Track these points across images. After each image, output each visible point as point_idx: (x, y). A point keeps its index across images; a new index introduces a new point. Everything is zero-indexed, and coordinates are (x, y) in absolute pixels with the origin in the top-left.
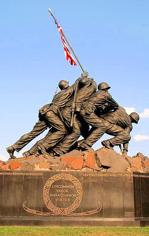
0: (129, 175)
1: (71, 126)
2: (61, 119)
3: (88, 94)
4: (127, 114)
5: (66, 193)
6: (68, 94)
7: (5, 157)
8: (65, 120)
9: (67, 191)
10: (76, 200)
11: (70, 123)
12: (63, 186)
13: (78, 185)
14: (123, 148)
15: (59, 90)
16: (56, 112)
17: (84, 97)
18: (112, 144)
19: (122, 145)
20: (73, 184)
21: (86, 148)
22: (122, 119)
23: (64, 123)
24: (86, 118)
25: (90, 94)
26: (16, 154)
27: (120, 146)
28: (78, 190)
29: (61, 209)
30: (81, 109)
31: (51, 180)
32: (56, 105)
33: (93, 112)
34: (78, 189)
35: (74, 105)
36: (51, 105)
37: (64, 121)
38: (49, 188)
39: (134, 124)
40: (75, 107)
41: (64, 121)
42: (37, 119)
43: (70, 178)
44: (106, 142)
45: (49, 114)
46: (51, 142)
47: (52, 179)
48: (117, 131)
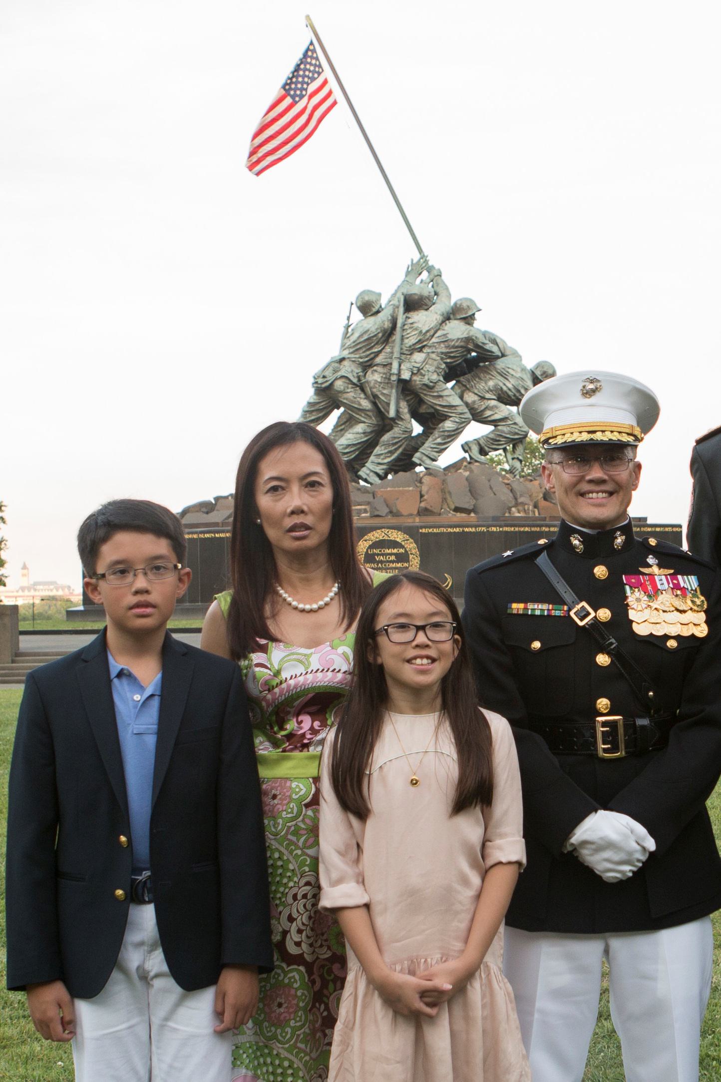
1: (392, 414)
2: (367, 397)
3: (427, 331)
4: (524, 369)
5: (393, 562)
6: (380, 335)
8: (375, 396)
9: (393, 558)
11: (388, 404)
12: (387, 551)
13: (411, 546)
15: (357, 316)
16: (355, 380)
17: (420, 340)
18: (487, 449)
19: (510, 448)
20: (402, 547)
22: (510, 386)
23: (374, 404)
24: (425, 395)
25: (432, 332)
27: (505, 450)
28: (411, 557)
30: (413, 374)
32: (354, 361)
33: (442, 379)
35: (395, 365)
36: (342, 360)
37: (374, 399)
40: (400, 366)
41: (374, 399)
42: (308, 394)
44: (471, 445)
45: (339, 385)
46: (347, 450)
48: (497, 417)
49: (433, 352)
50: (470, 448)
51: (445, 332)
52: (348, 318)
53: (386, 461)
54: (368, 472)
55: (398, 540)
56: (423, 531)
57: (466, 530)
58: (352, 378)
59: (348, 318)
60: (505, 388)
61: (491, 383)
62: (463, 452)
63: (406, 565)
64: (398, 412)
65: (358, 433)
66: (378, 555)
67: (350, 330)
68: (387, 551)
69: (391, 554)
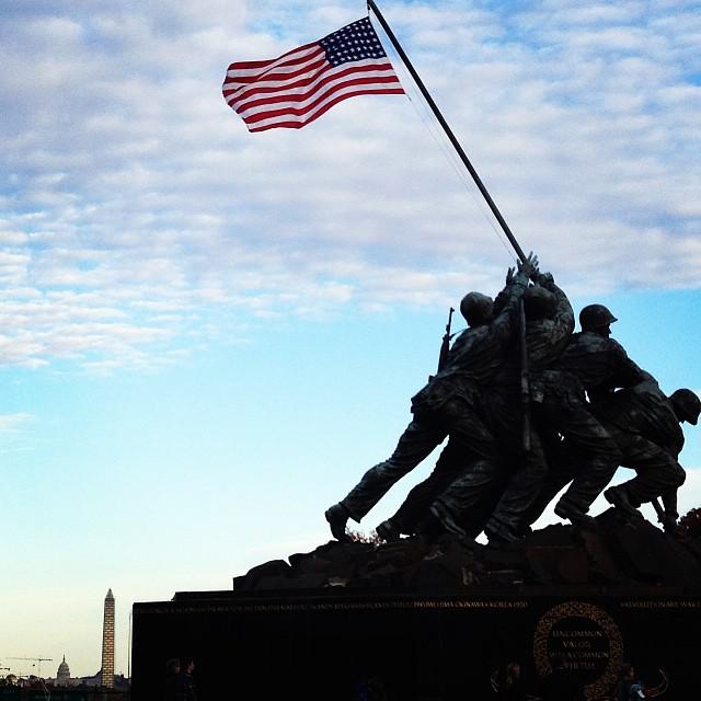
3: (557, 343)
7: (324, 535)
13: (610, 626)
20: (599, 628)
31: (549, 618)
35: (525, 384)
39: (685, 426)
43: (593, 613)
48: (647, 456)
49: (569, 370)
51: (581, 344)
52: (448, 328)
53: (518, 510)
54: (498, 525)
55: (593, 617)
58: (469, 400)
59: (448, 328)
60: (650, 420)
61: (633, 413)
62: (607, 502)
64: (531, 446)
65: (478, 472)
66: (565, 639)
67: (452, 343)
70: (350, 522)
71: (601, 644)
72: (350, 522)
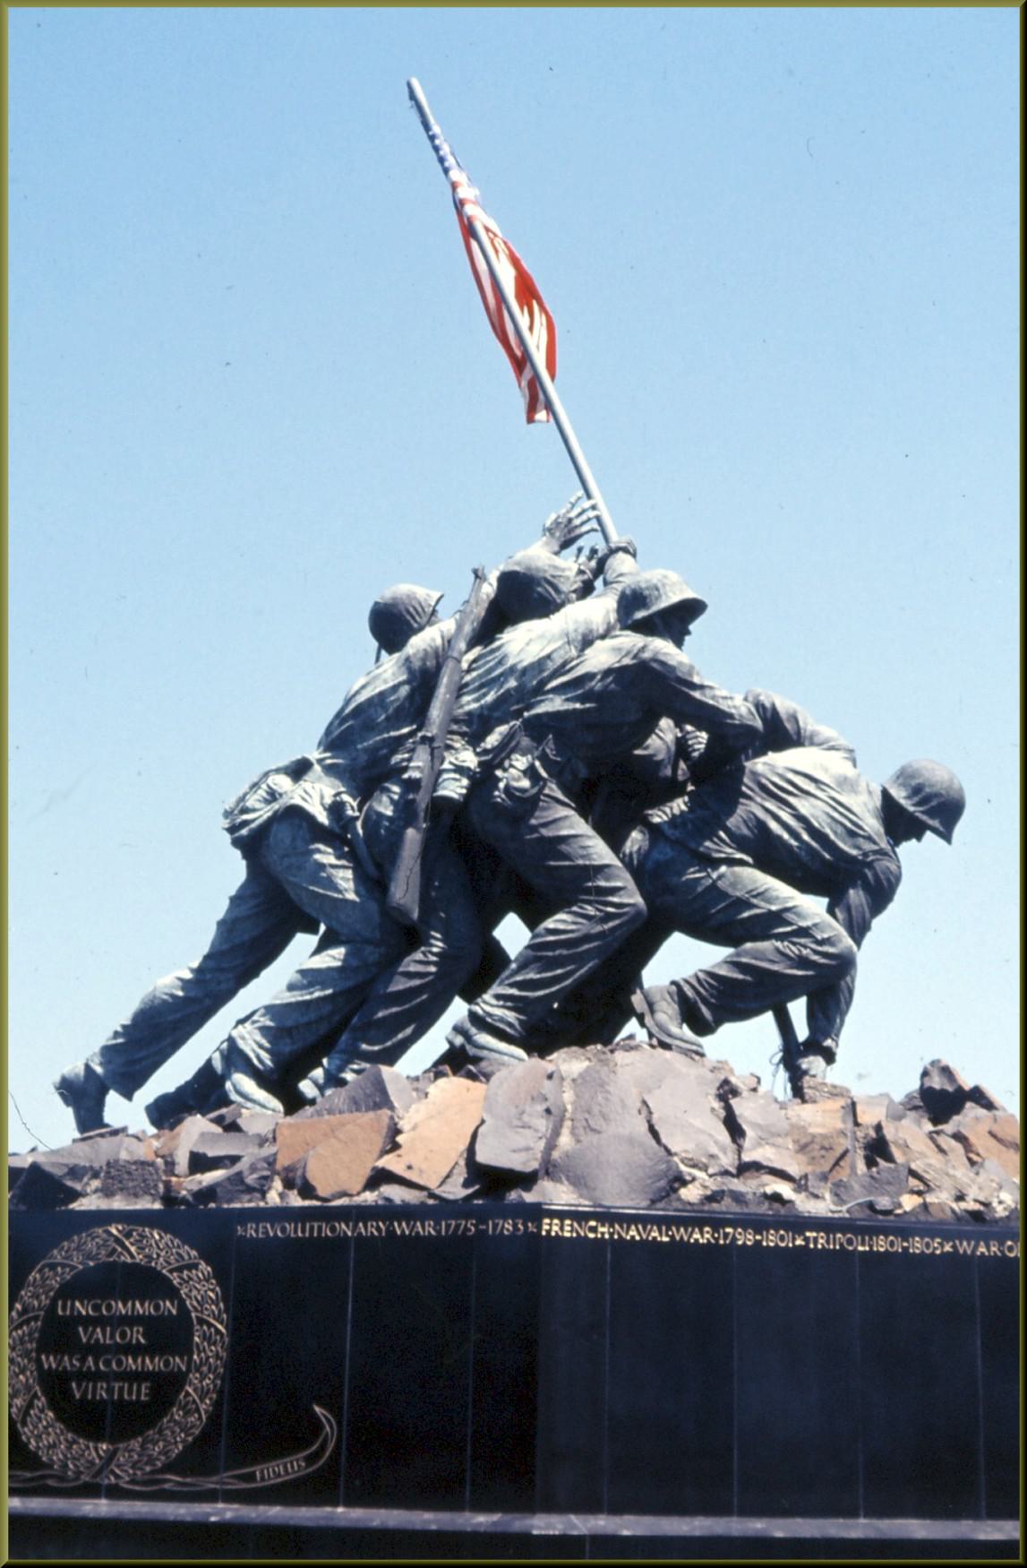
0: (515, 1225)
5: (135, 1350)
9: (137, 1335)
10: (188, 1394)
12: (121, 1308)
13: (201, 1290)
14: (802, 1032)
20: (172, 1293)
21: (471, 1051)
26: (117, 1109)
29: (96, 1449)
34: (201, 1321)
36: (299, 770)
38: (36, 1318)
43: (161, 1249)
44: (656, 998)
47: (59, 1259)
50: (651, 1005)
55: (160, 1265)
56: (251, 1232)
57: (401, 1228)
63: (178, 1362)
66: (87, 1322)
68: (121, 1308)
69: (132, 1320)
70: (113, 1099)
71: (171, 1334)
72: (113, 1099)
